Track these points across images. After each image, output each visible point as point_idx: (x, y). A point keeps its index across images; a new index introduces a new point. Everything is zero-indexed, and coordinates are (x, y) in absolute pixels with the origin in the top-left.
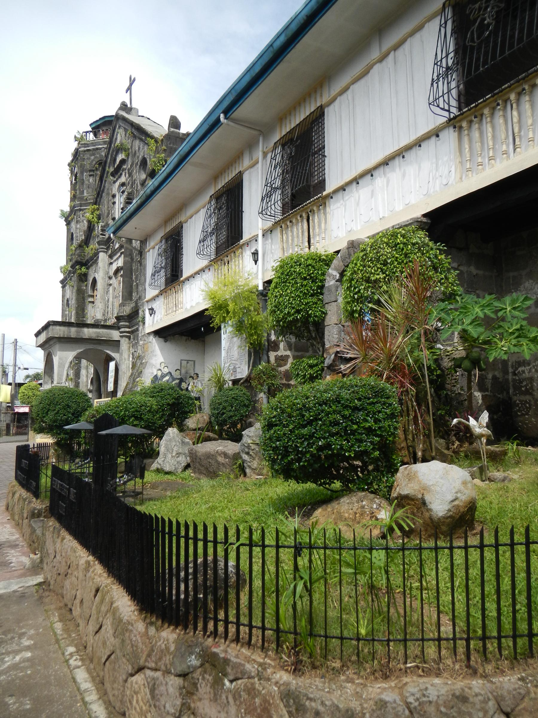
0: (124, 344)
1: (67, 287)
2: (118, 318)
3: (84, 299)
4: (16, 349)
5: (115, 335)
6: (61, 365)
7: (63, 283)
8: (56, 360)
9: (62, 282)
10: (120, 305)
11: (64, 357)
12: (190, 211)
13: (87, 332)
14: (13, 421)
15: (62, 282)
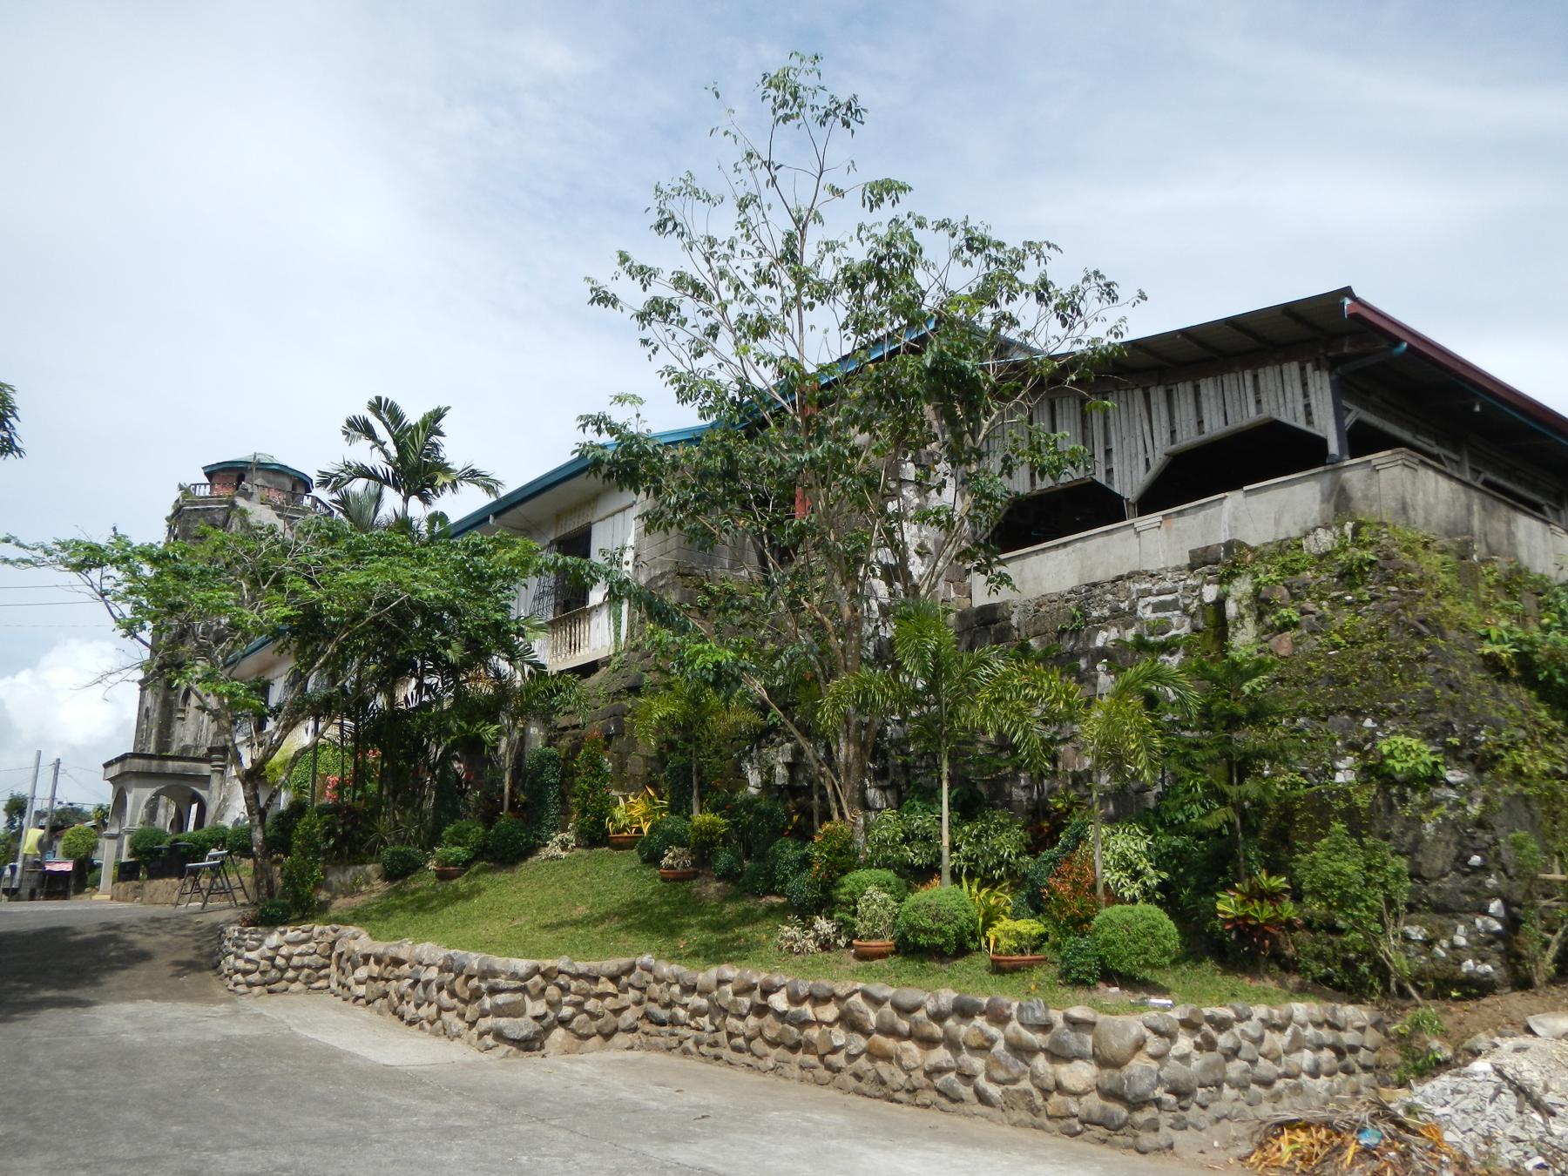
0: (215, 781)
1: (148, 692)
2: (211, 750)
3: (171, 713)
4: (56, 774)
5: (206, 769)
6: (136, 805)
7: (144, 684)
8: (130, 798)
9: (141, 682)
10: (215, 735)
11: (138, 796)
12: (277, 673)
13: (172, 766)
14: (41, 884)
15: (141, 682)
